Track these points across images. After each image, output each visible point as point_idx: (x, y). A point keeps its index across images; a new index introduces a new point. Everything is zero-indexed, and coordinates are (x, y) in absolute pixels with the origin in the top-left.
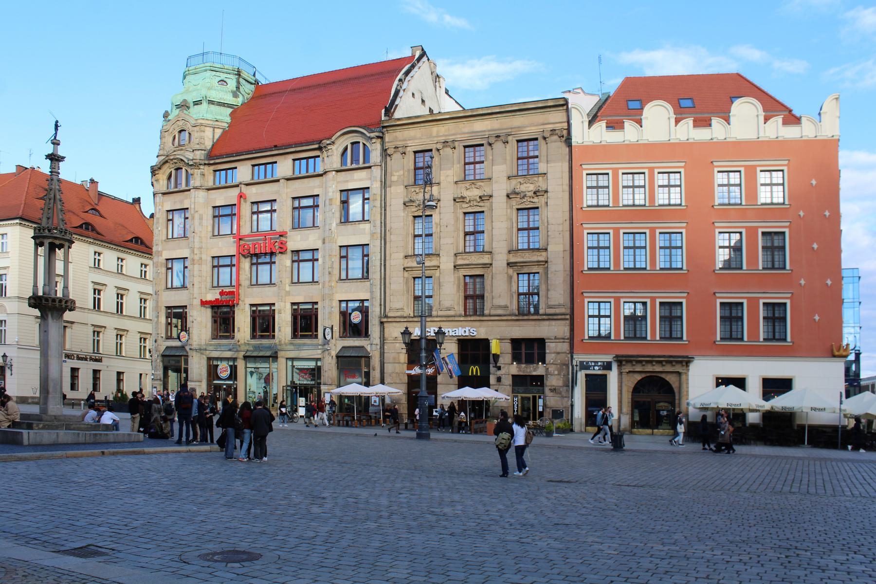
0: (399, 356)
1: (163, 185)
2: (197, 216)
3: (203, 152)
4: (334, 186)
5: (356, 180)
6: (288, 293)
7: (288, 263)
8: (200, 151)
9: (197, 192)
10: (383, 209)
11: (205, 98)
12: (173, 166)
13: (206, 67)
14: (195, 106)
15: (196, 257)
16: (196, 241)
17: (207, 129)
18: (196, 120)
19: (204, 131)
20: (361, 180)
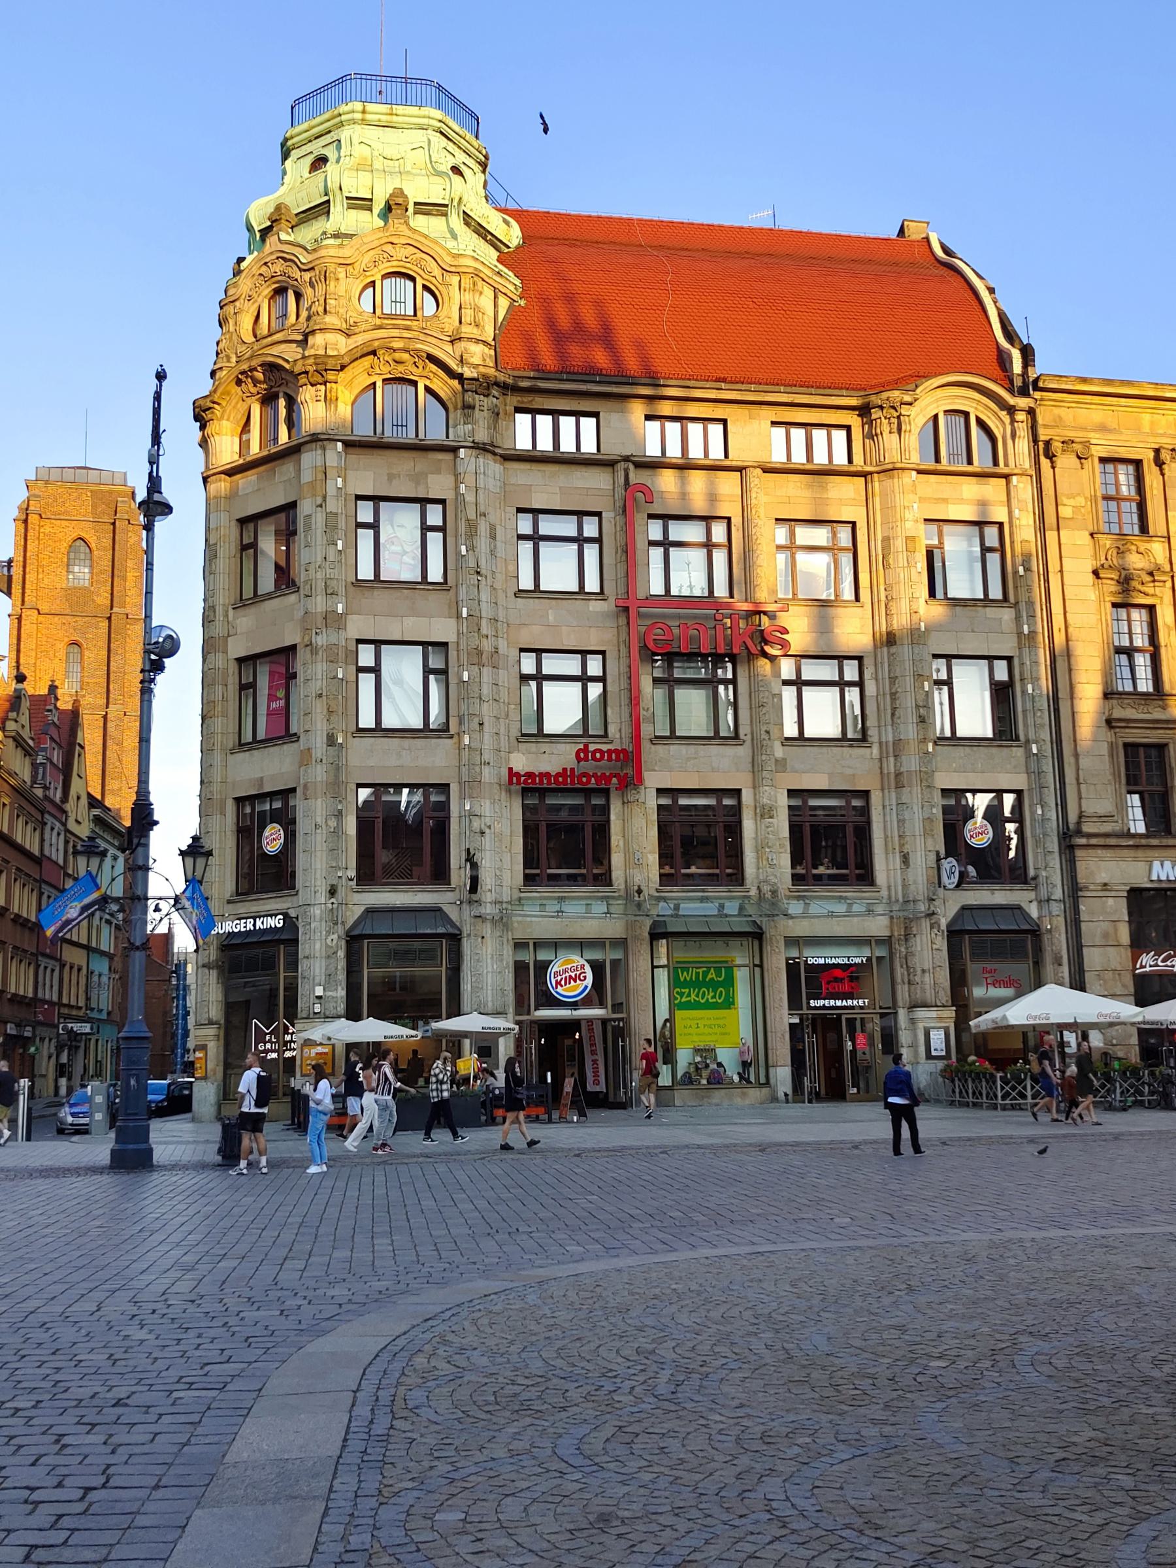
0: (1116, 930)
6: (781, 764)
9: (481, 460)
11: (455, 203)
12: (385, 369)
15: (487, 645)
16: (484, 597)
19: (481, 293)
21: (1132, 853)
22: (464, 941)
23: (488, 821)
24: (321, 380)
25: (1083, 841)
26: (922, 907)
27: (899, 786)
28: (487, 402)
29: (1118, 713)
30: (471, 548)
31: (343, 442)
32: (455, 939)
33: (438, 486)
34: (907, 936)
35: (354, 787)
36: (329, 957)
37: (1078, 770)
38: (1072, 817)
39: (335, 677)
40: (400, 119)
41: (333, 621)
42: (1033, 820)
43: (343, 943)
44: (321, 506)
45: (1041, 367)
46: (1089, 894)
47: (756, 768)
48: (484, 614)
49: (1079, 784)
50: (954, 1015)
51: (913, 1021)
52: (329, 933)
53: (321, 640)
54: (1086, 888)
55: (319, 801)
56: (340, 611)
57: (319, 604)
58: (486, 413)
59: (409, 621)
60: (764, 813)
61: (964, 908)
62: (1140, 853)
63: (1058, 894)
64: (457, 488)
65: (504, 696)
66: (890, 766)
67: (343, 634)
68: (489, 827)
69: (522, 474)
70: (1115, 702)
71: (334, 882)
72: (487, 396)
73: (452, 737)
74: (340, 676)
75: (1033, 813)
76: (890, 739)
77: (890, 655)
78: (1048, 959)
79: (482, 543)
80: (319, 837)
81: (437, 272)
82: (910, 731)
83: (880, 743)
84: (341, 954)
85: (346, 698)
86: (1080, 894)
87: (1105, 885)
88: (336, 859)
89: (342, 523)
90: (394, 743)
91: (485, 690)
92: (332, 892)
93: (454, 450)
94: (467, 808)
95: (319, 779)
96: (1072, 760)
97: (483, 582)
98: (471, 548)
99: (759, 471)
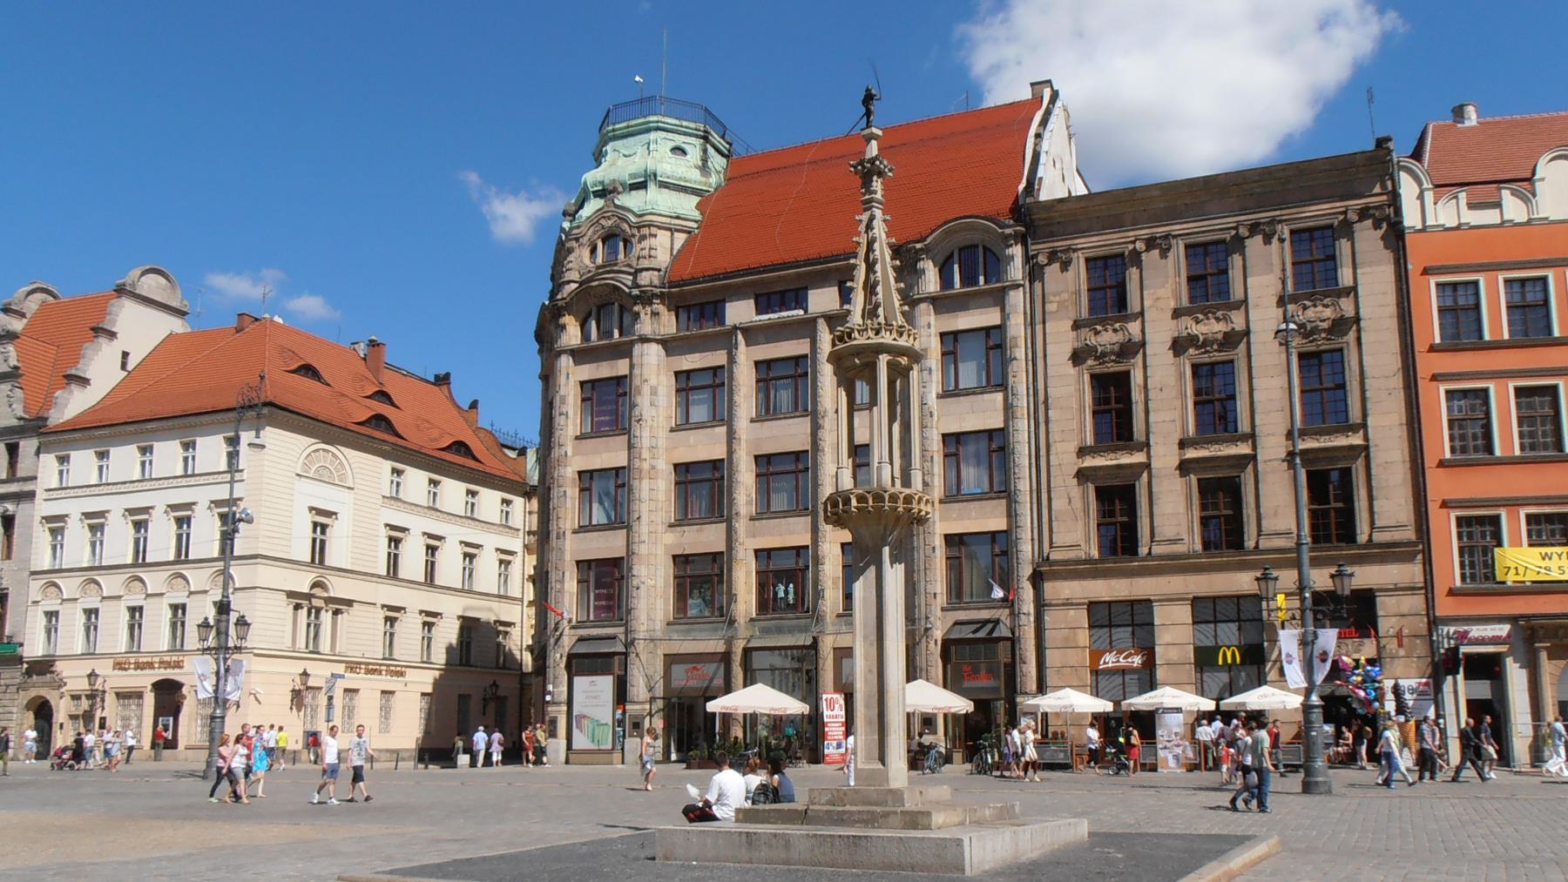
2: (646, 390)
3: (656, 273)
8: (651, 272)
17: (661, 233)
19: (655, 236)
48: (644, 446)
81: (628, 230)
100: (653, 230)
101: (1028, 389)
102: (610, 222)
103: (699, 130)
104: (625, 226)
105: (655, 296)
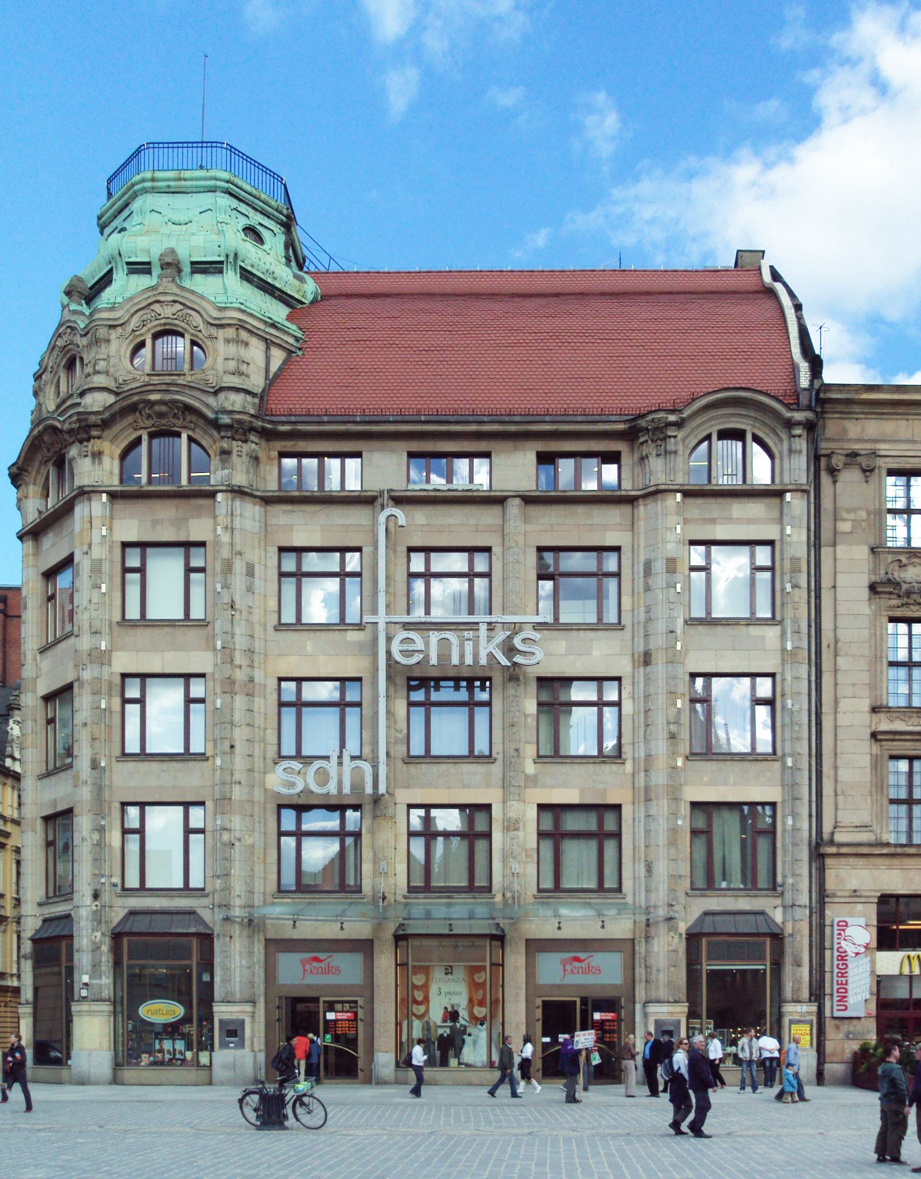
1: (111, 473)
4: (679, 531)
5: (739, 521)
6: (532, 781)
7: (531, 706)
9: (238, 503)
10: (813, 594)
13: (216, 179)
14: (198, 277)
15: (240, 675)
16: (237, 631)
18: (222, 309)
20: (750, 521)
21: (887, 861)
22: (215, 939)
23: (238, 835)
24: (85, 436)
25: (833, 850)
26: (662, 912)
27: (648, 800)
28: (246, 448)
29: (885, 726)
30: (226, 586)
31: (108, 493)
32: (207, 939)
33: (197, 530)
34: (647, 938)
35: (118, 805)
36: (93, 951)
37: (836, 781)
38: (827, 828)
39: (98, 708)
40: (189, 183)
41: (101, 658)
42: (784, 831)
43: (107, 940)
44: (87, 553)
45: (830, 376)
46: (836, 900)
47: (505, 785)
48: (237, 647)
49: (836, 795)
50: (686, 1010)
51: (646, 1015)
52: (93, 930)
53: (86, 675)
54: (834, 896)
55: (85, 818)
56: (103, 648)
57: (85, 643)
58: (245, 459)
59: (170, 656)
60: (511, 826)
61: (706, 914)
62: (896, 861)
63: (804, 899)
64: (215, 530)
65: (259, 721)
66: (641, 781)
67: (106, 669)
68: (239, 840)
69: (281, 516)
70: (882, 716)
71: (98, 887)
72: (246, 441)
73: (207, 759)
74: (103, 706)
75: (784, 824)
76: (642, 755)
77: (645, 674)
78: (788, 959)
79: (238, 580)
80: (85, 849)
82: (660, 747)
83: (634, 759)
84: (105, 948)
85: (109, 727)
86: (827, 900)
87: (855, 891)
88: (100, 869)
89: (106, 567)
90: (154, 766)
91: (238, 716)
92: (96, 896)
93: (212, 495)
94: (218, 822)
95: (84, 798)
96: (832, 772)
97: (237, 616)
98: (226, 586)
99: (517, 501)
100: (244, 335)
101: (809, 626)
102: (168, 311)
103: (280, 213)
104: (197, 320)
105: (252, 429)
